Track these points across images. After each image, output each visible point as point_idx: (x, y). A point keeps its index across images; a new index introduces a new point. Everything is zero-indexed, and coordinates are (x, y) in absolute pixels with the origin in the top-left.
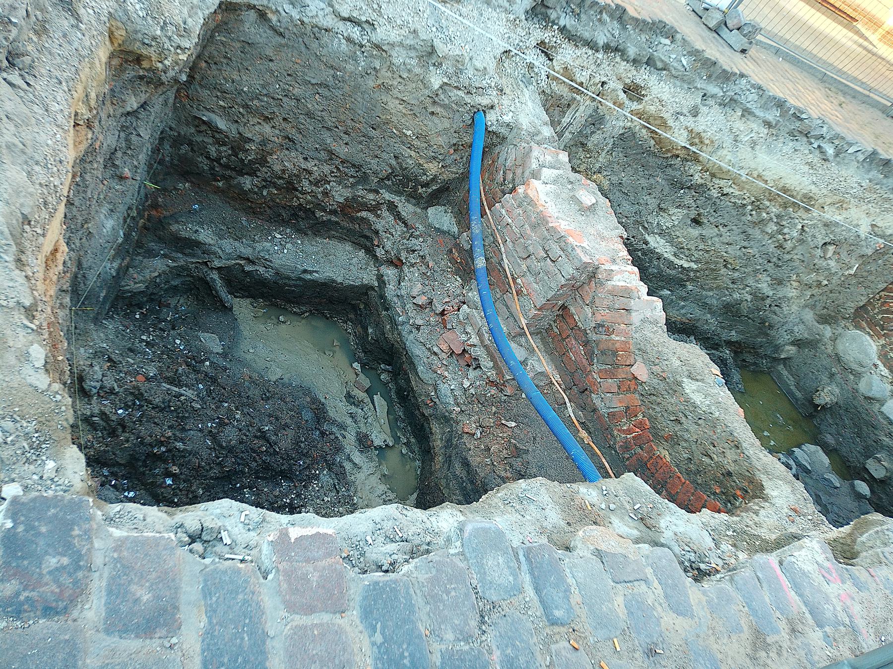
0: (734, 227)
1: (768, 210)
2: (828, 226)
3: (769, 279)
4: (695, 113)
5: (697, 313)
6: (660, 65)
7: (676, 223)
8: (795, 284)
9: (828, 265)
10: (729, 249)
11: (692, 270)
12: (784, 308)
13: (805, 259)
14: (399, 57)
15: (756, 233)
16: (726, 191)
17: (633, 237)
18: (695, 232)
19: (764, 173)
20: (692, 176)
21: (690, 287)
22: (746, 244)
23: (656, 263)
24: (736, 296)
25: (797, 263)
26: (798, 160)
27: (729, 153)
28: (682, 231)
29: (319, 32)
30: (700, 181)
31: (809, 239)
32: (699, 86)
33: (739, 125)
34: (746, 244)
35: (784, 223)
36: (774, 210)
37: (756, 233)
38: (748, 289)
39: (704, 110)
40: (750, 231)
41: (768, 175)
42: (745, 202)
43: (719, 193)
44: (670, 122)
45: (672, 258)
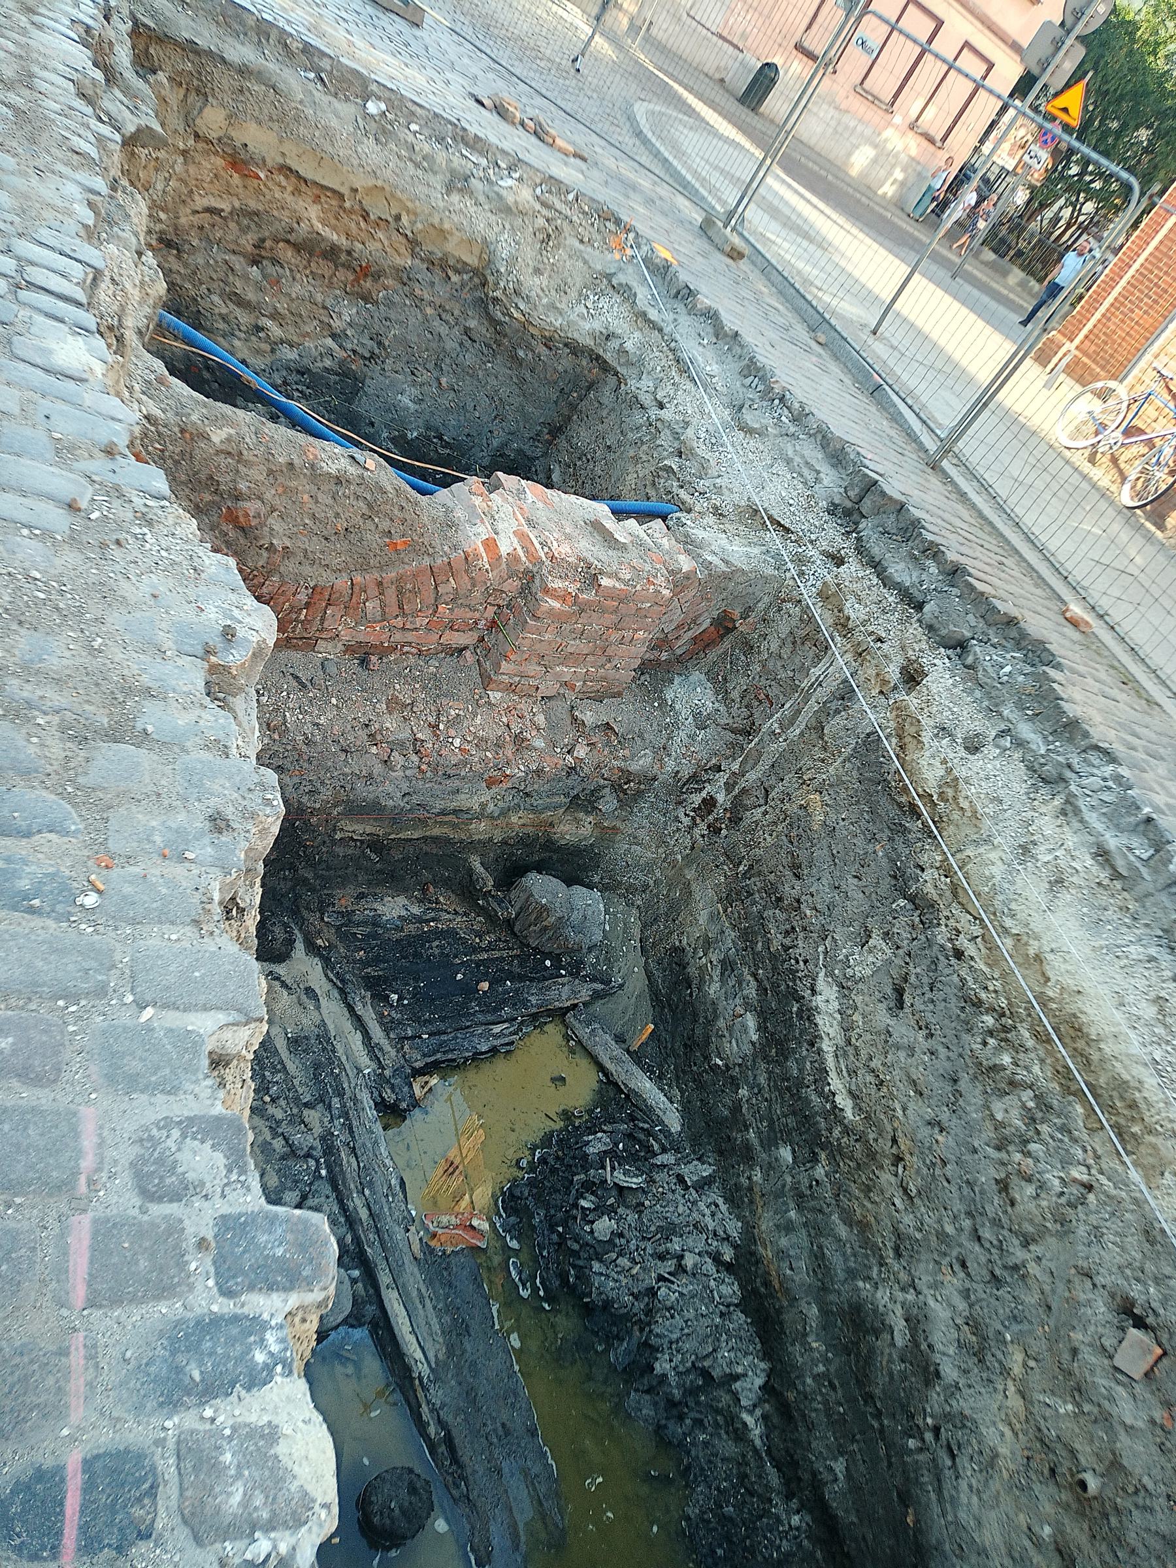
0: (942, 1051)
1: (1021, 1056)
2: (1152, 1242)
3: (962, 1305)
4: (973, 746)
5: (800, 1273)
6: (970, 660)
7: (868, 972)
8: (1015, 1402)
9: (1111, 1399)
10: (911, 1106)
11: (840, 1121)
12: (963, 1485)
13: (1054, 1306)
14: (665, 439)
15: (973, 1094)
16: (963, 942)
17: (805, 962)
18: (882, 1017)
19: (1050, 957)
20: (923, 870)
21: (820, 1172)
22: (945, 1115)
23: (805, 1053)
24: (882, 1296)
25: (1031, 1299)
26: (1141, 983)
27: (999, 863)
28: (867, 999)
29: (635, 403)
30: (929, 888)
31: (1082, 1231)
32: (1006, 713)
33: (1047, 825)
34: (945, 1115)
35: (1044, 1128)
36: (1036, 1069)
37: (973, 1094)
38: (910, 1296)
39: (991, 751)
40: (964, 1084)
41: (1056, 967)
42: (983, 995)
43: (950, 940)
44: (926, 737)
45: (830, 1062)
